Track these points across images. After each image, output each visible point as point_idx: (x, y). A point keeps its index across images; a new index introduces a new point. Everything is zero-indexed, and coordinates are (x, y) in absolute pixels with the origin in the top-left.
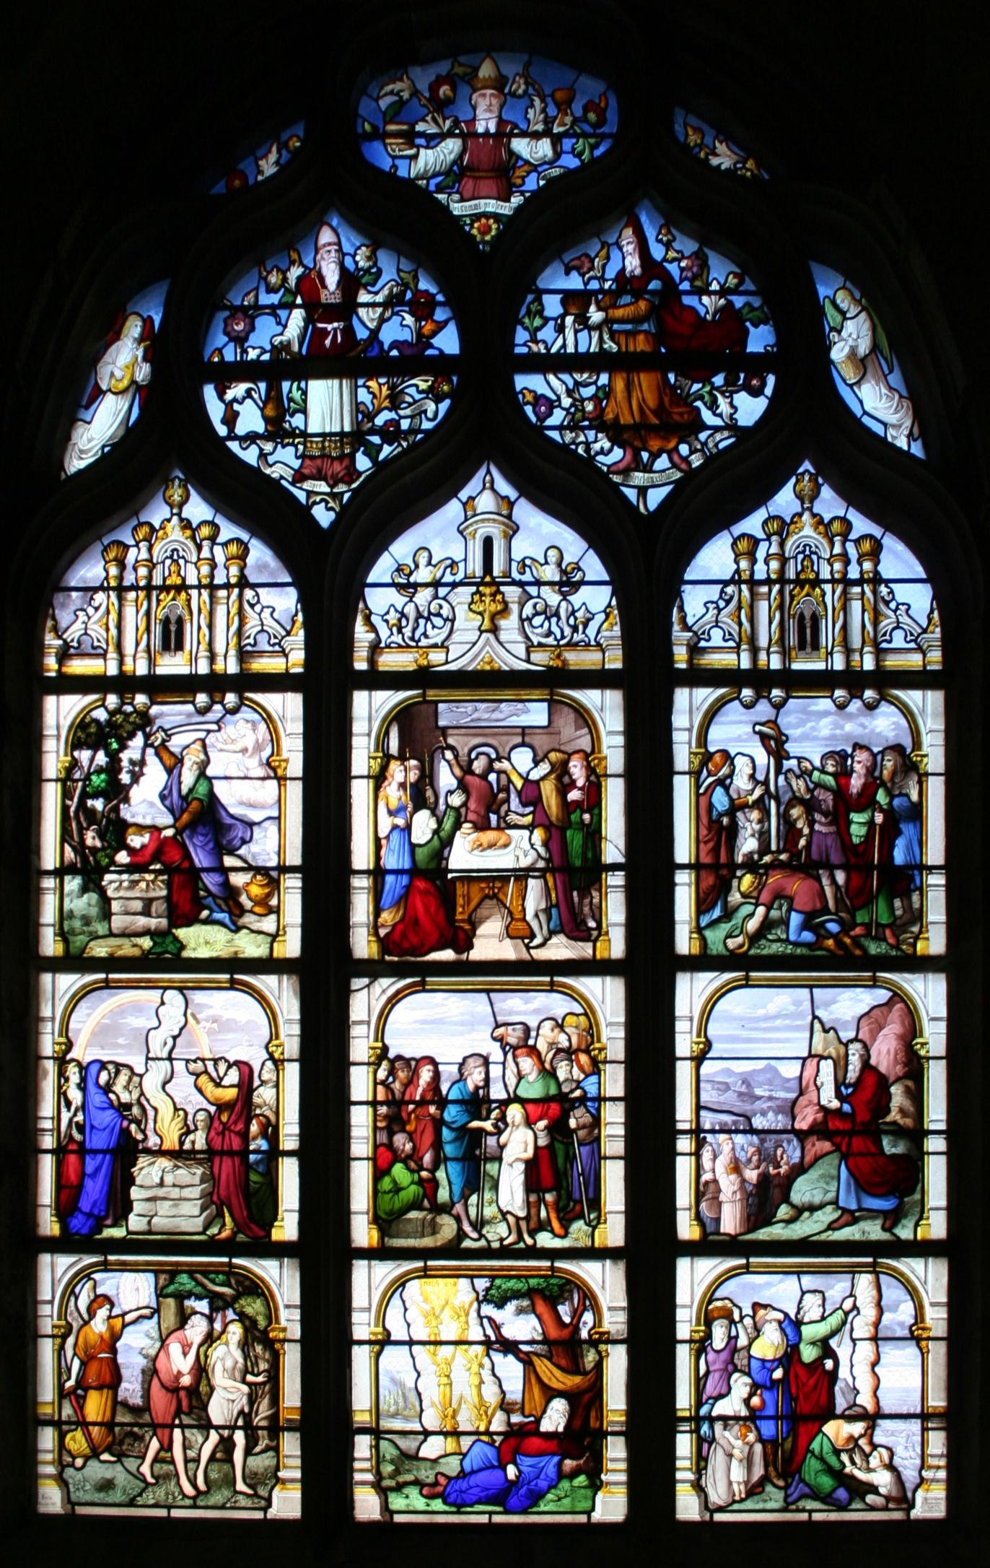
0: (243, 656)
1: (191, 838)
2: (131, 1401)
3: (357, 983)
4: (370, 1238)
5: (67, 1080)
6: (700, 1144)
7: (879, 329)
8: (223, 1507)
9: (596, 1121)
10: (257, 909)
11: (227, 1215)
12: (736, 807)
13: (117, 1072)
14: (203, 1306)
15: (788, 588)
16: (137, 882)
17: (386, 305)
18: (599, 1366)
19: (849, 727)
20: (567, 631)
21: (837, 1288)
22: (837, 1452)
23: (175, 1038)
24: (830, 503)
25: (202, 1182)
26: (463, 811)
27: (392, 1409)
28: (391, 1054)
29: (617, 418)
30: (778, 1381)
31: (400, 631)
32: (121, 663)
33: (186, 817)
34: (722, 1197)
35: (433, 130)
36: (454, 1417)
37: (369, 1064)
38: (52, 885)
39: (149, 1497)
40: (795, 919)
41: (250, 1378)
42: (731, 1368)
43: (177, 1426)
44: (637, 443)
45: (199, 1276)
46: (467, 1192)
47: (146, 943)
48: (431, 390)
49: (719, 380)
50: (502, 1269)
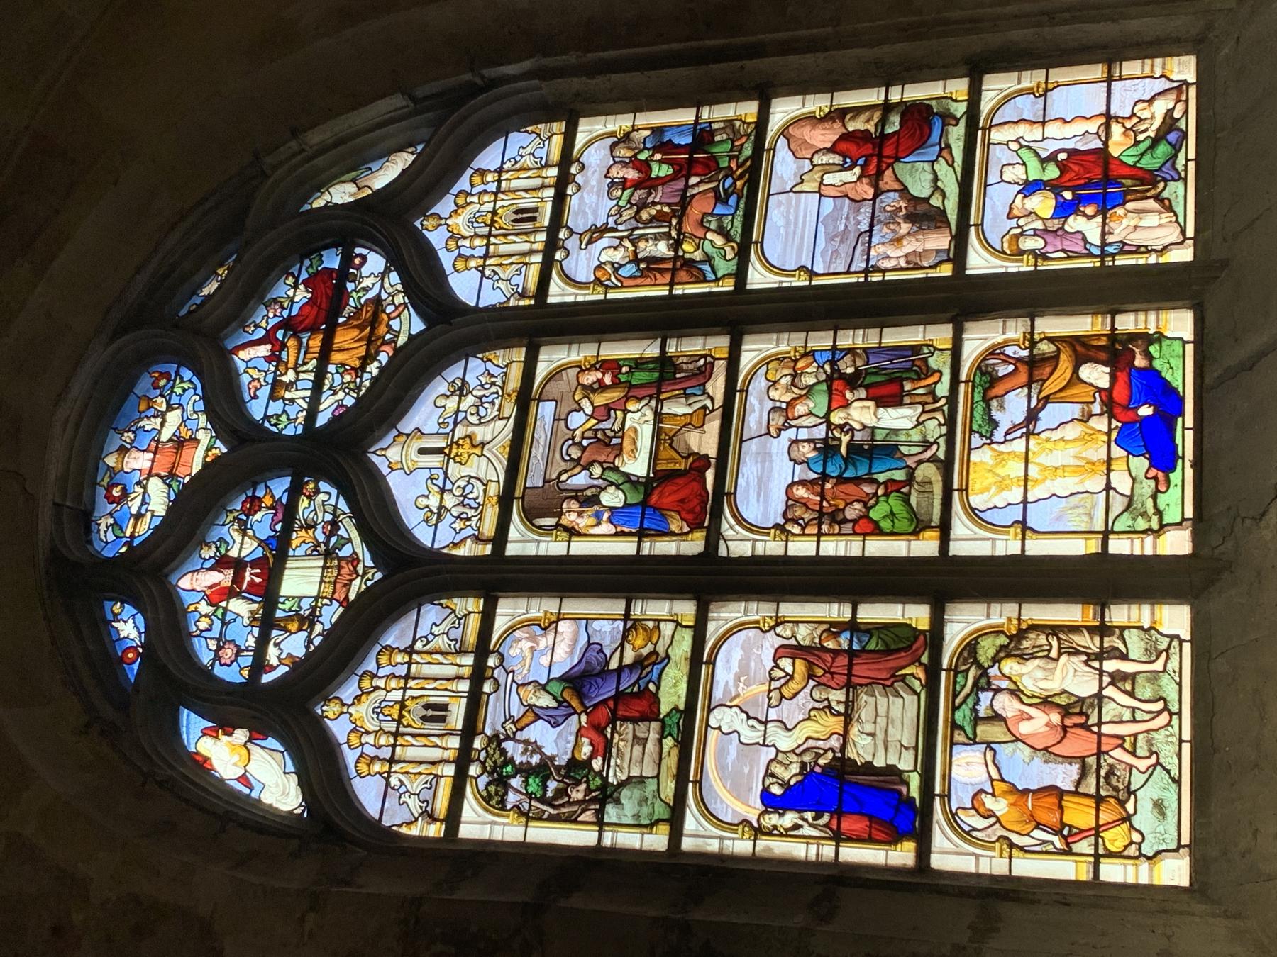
0: (461, 652)
1: (592, 699)
2: (1076, 777)
3: (722, 552)
4: (931, 538)
5: (775, 827)
6: (877, 269)
7: (343, 178)
8: (1180, 684)
9: (850, 351)
10: (654, 640)
11: (903, 672)
12: (636, 260)
13: (773, 775)
14: (985, 697)
15: (494, 232)
16: (618, 750)
17: (244, 534)
18: (1051, 340)
19: (593, 183)
20: (494, 389)
21: (999, 155)
22: (1137, 143)
23: (749, 717)
24: (444, 207)
25: (873, 695)
26: (605, 465)
27: (1086, 519)
28: (781, 521)
29: (359, 358)
30: (1074, 195)
31: (469, 519)
32: (447, 761)
33: (575, 703)
34: (920, 249)
35: (138, 501)
36: (1094, 464)
38: (610, 834)
39: (1171, 762)
40: (720, 210)
41: (1054, 654)
42: (1060, 233)
43: (1100, 728)
44: (379, 343)
45: (958, 701)
46: (898, 455)
47: (668, 742)
48: (309, 497)
49: (350, 286)
50: (964, 424)
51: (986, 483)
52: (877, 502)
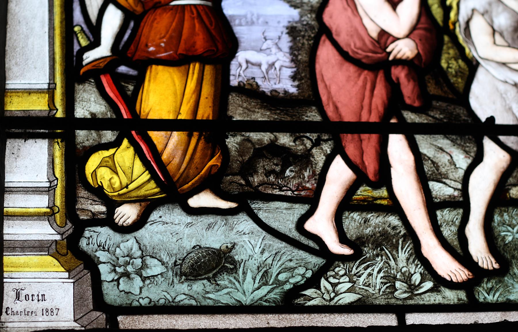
2: (266, 86)
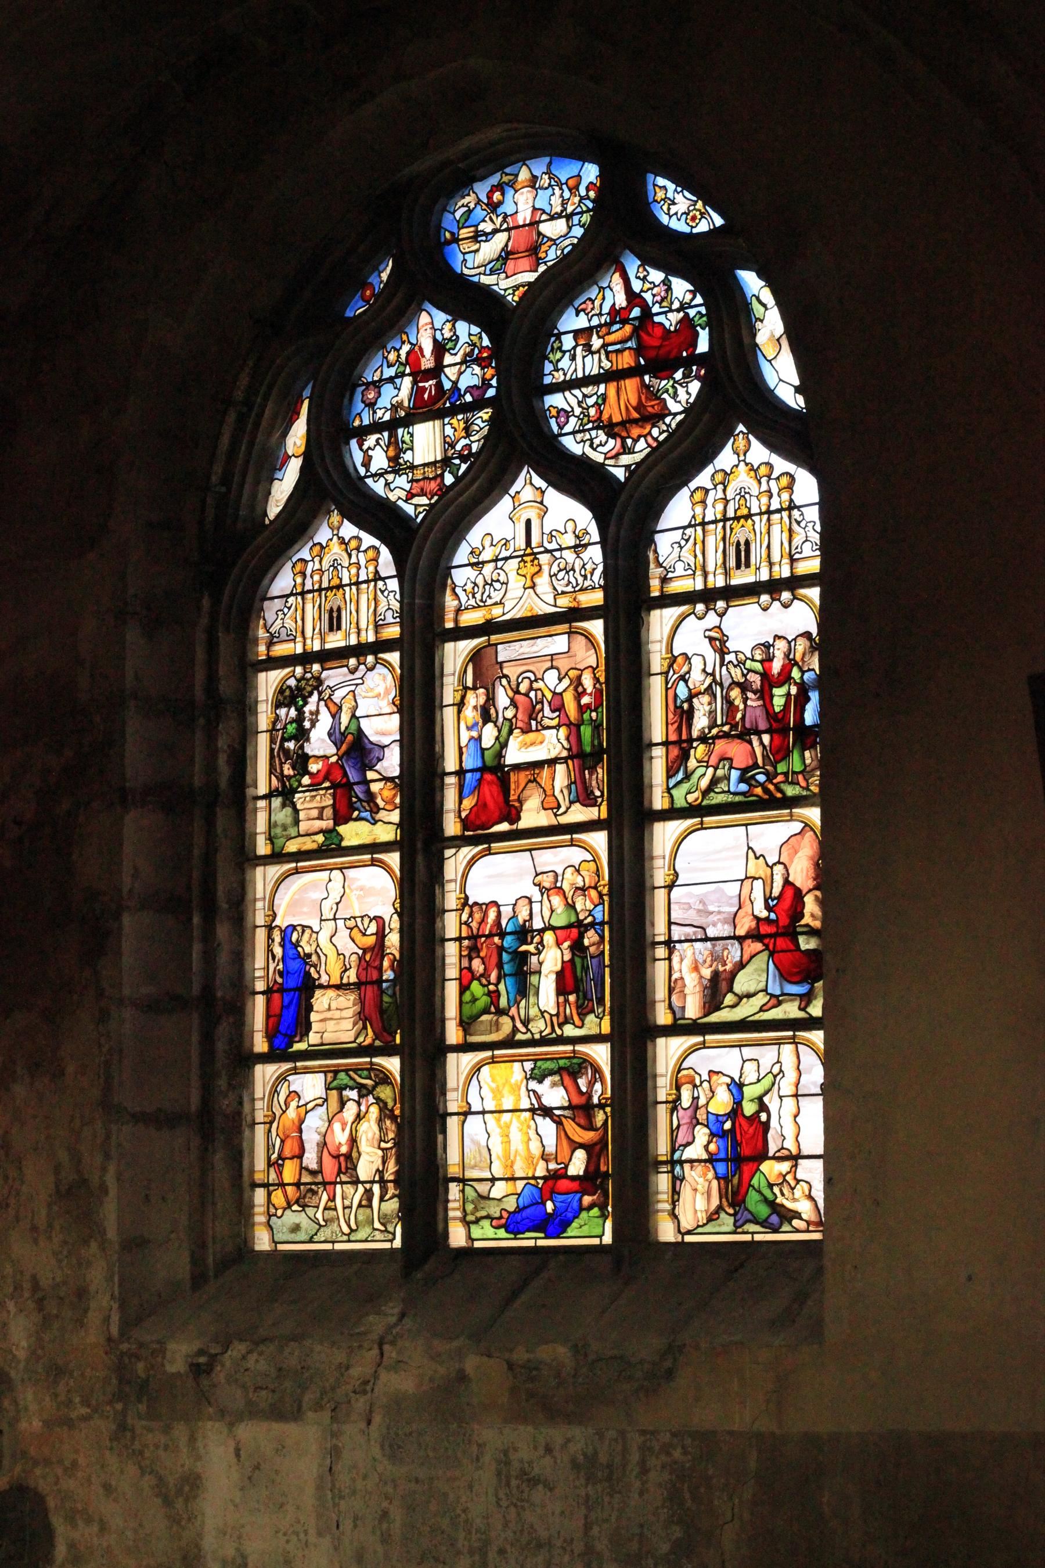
4: (458, 1037)
8: (366, 1241)
25: (354, 1005)
28: (470, 902)
37: (456, 910)
41: (383, 1145)
42: (695, 1122)
45: (351, 1073)
46: (519, 998)
51: (498, 1078)
52: (484, 986)
